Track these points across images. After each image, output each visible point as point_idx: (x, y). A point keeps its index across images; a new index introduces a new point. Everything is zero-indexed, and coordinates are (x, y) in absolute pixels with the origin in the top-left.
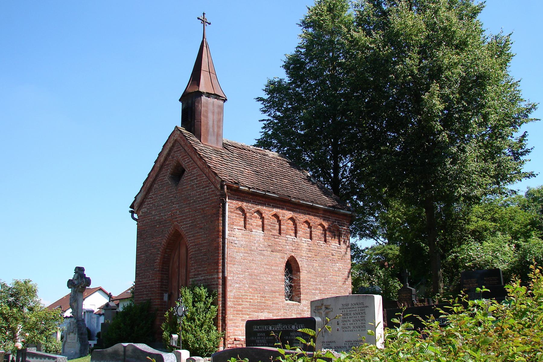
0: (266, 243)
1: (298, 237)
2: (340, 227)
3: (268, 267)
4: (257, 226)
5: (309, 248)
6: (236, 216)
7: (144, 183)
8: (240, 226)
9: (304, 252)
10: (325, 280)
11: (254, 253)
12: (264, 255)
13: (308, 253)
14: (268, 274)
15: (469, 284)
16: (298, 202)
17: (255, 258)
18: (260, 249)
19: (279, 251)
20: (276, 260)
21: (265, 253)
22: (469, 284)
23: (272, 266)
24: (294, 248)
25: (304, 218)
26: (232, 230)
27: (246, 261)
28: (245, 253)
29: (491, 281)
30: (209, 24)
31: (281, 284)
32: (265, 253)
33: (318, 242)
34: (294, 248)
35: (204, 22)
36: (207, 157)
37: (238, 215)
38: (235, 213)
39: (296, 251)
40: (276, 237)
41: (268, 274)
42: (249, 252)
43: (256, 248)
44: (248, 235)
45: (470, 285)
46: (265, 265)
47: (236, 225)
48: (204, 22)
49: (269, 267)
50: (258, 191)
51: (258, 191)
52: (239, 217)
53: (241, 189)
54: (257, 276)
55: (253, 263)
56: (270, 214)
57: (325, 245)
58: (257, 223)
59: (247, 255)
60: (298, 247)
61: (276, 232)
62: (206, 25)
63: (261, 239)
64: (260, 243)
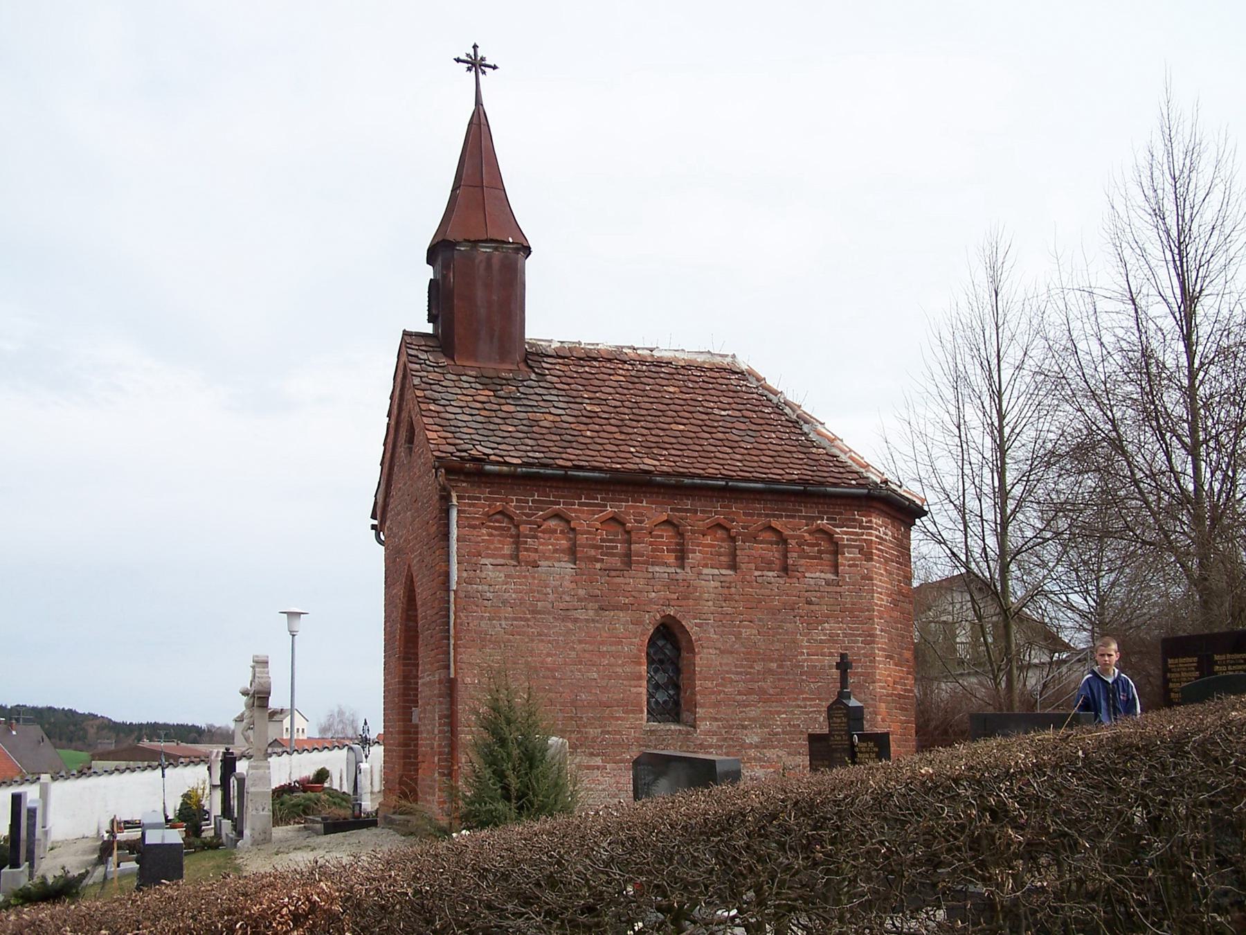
0: (582, 592)
1: (688, 570)
2: (838, 530)
3: (587, 647)
4: (555, 551)
5: (726, 591)
6: (490, 535)
7: (385, 444)
8: (503, 556)
9: (710, 603)
10: (780, 666)
11: (544, 618)
12: (576, 620)
13: (724, 605)
14: (589, 663)
15: (1180, 672)
16: (677, 481)
17: (549, 628)
18: (562, 605)
19: (624, 608)
20: (616, 629)
21: (580, 614)
22: (1180, 672)
23: (602, 643)
24: (675, 596)
25: (709, 518)
26: (474, 568)
27: (518, 637)
28: (515, 619)
29: (1232, 665)
30: (495, 68)
31: (631, 686)
32: (580, 614)
33: (757, 573)
34: (675, 596)
35: (476, 64)
36: (434, 400)
37: (495, 532)
38: (489, 527)
39: (684, 603)
40: (613, 573)
41: (589, 663)
42: (529, 616)
43: (551, 606)
44: (525, 577)
45: (1183, 674)
46: (580, 642)
47: (488, 556)
48: (476, 64)
49: (591, 648)
50: (542, 471)
51: (542, 471)
52: (499, 535)
53: (489, 470)
54: (552, 670)
55: (542, 641)
56: (596, 520)
57: (781, 581)
58: (557, 544)
59: (523, 623)
60: (686, 592)
61: (616, 562)
62: (484, 72)
63: (566, 583)
64: (564, 593)
